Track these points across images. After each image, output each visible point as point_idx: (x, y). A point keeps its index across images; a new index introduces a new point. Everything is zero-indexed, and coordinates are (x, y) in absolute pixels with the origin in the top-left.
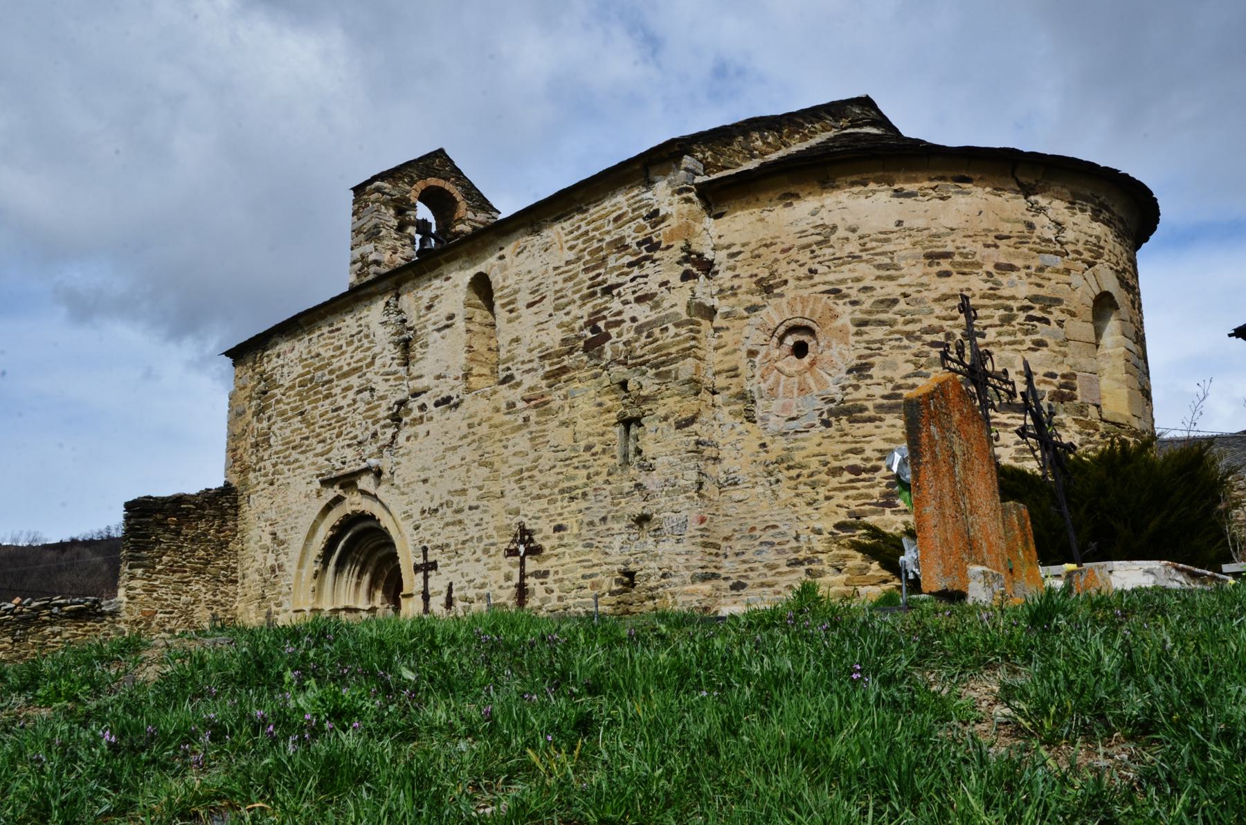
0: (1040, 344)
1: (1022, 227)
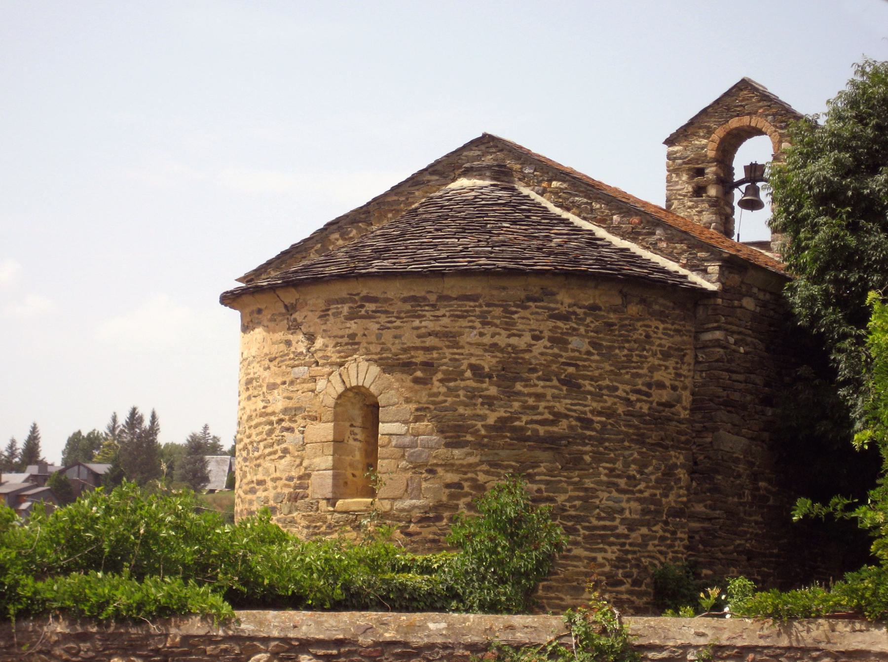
0: (286, 451)
1: (283, 347)
